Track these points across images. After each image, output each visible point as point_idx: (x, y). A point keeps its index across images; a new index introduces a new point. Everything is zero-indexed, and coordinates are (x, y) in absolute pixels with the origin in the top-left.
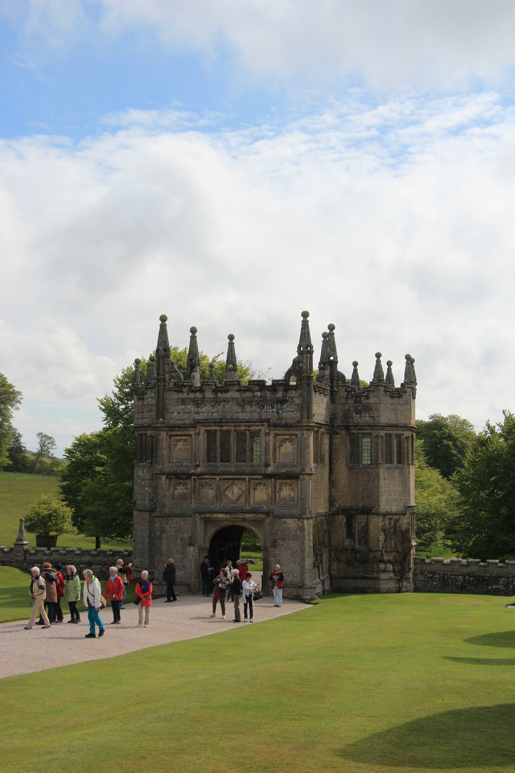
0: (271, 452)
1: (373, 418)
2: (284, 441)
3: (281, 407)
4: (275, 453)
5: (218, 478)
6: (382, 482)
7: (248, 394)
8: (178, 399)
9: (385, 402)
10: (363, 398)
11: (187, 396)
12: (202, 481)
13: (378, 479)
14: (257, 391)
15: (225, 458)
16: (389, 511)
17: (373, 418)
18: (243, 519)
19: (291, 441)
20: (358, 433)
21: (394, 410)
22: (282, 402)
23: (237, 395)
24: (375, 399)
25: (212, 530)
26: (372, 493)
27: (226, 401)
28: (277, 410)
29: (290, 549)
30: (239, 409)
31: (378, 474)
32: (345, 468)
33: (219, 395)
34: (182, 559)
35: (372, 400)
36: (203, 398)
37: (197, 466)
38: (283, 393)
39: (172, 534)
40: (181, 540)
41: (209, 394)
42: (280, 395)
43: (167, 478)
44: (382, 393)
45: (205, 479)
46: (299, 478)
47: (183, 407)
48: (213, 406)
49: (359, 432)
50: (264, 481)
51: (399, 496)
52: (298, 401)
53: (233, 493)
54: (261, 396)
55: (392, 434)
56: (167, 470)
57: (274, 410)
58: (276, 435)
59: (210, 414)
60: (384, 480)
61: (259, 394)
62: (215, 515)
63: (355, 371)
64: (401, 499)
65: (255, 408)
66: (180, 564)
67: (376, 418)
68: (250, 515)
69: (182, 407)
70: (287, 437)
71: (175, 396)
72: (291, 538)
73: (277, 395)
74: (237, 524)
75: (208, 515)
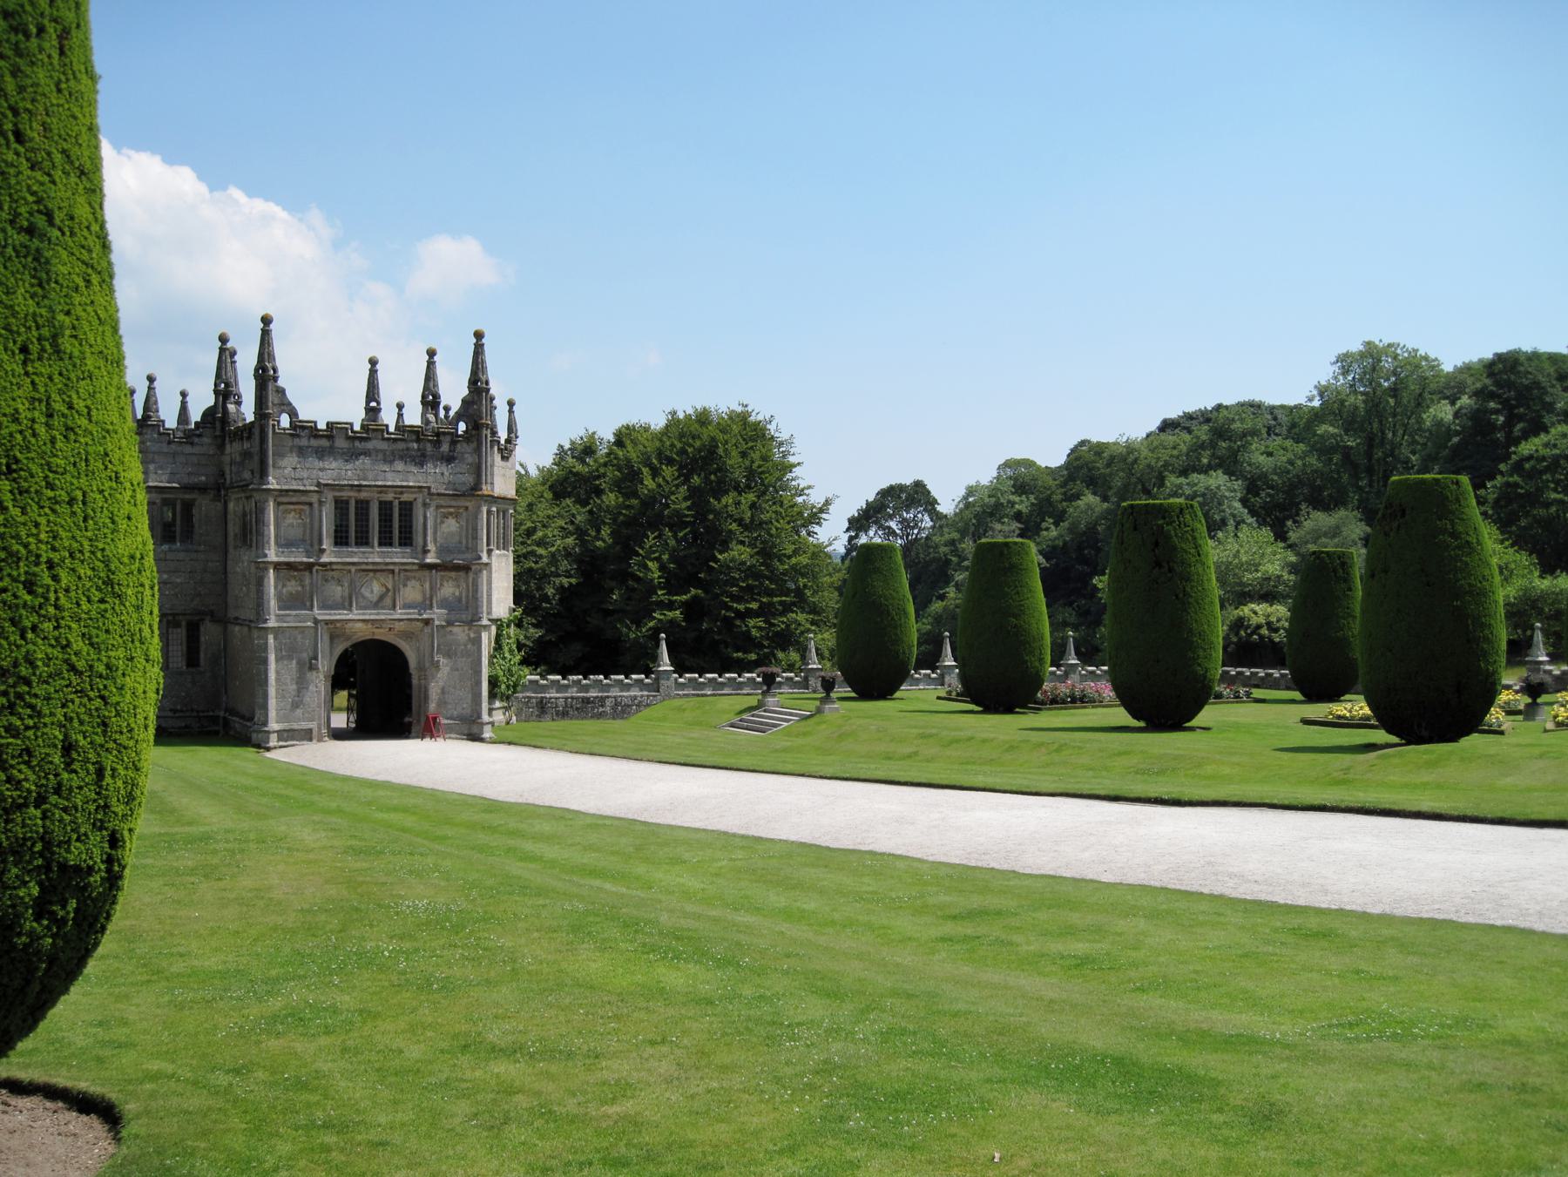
2: (446, 516)
4: (435, 533)
5: (353, 569)
19: (457, 516)
23: (383, 446)
33: (357, 443)
36: (332, 447)
37: (322, 551)
41: (341, 443)
42: (445, 448)
50: (418, 574)
52: (469, 459)
58: (438, 507)
61: (415, 445)
63: (400, 415)
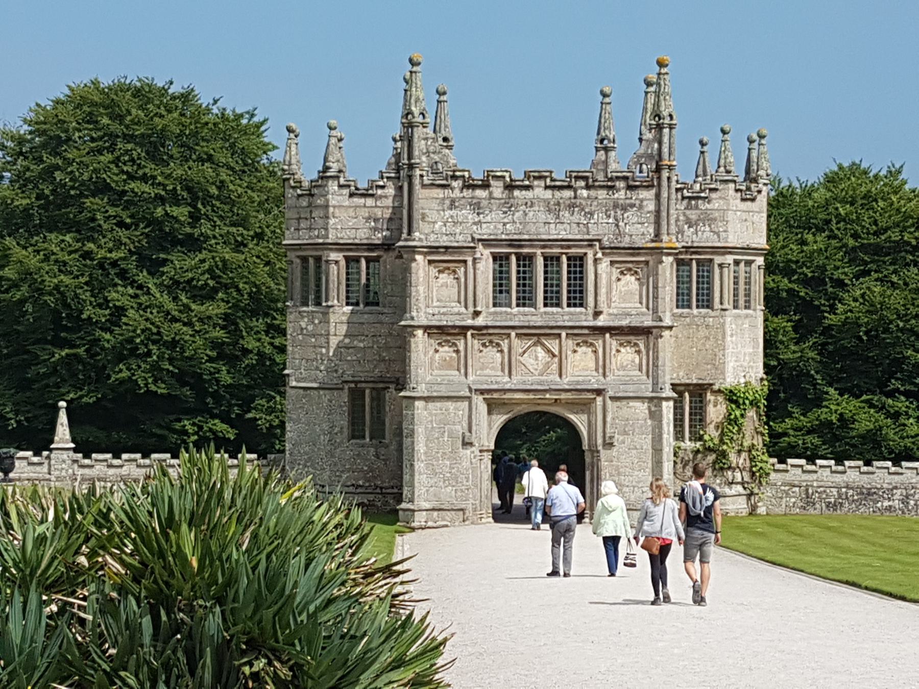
6: (729, 339)
7: (568, 193)
8: (444, 199)
10: (700, 202)
13: (724, 337)
14: (582, 188)
20: (692, 259)
23: (548, 194)
24: (722, 202)
25: (500, 420)
28: (616, 220)
30: (551, 218)
35: (715, 205)
37: (477, 314)
43: (425, 332)
44: (732, 192)
46: (651, 333)
48: (505, 213)
49: (694, 257)
53: (537, 358)
55: (742, 260)
56: (425, 322)
59: (500, 226)
60: (732, 335)
62: (508, 396)
69: (451, 212)
70: (630, 265)
71: (439, 193)
72: (637, 430)
73: (616, 196)
75: (496, 396)
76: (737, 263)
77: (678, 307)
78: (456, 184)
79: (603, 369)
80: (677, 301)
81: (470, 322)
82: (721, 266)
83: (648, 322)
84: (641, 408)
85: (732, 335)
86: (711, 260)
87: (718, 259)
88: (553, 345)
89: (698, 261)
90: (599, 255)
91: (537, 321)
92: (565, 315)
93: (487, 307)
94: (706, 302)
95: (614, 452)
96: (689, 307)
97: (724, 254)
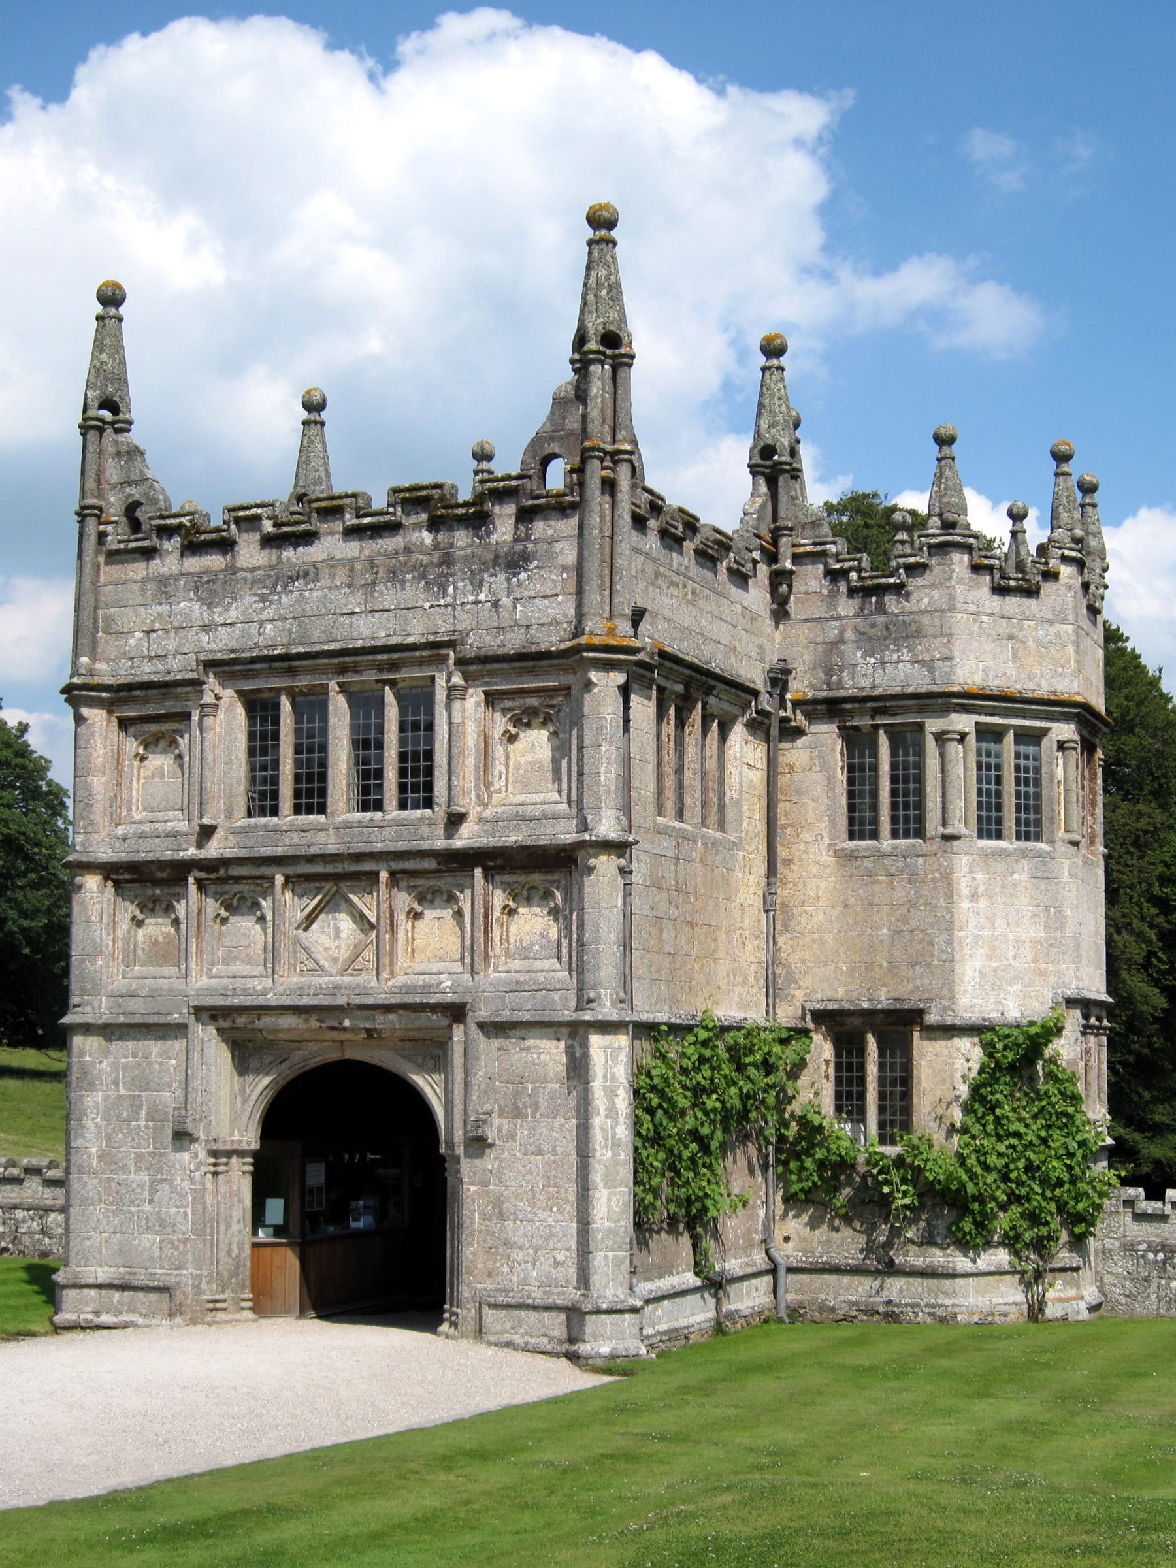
0: (470, 762)
1: (929, 665)
3: (508, 580)
6: (965, 905)
8: (145, 581)
9: (972, 608)
11: (175, 569)
12: (226, 888)
13: (950, 897)
15: (311, 797)
16: (994, 1015)
17: (929, 665)
18: (369, 1032)
20: (876, 727)
21: (1011, 637)
22: (515, 562)
23: (352, 549)
24: (935, 594)
26: (930, 944)
27: (308, 574)
29: (540, 1152)
30: (355, 602)
31: (947, 877)
32: (828, 858)
33: (288, 554)
34: (153, 1191)
36: (231, 570)
37: (207, 832)
38: (516, 527)
39: (122, 1091)
40: (150, 1117)
41: (250, 553)
43: (106, 879)
45: (238, 879)
46: (575, 862)
47: (164, 608)
48: (263, 598)
50: (444, 883)
51: (1035, 960)
53: (337, 933)
54: (436, 546)
55: (1007, 727)
56: (105, 854)
57: (482, 597)
60: (974, 896)
61: (427, 537)
62: (267, 1021)
64: (1042, 974)
65: (414, 593)
66: (147, 1207)
67: (938, 663)
68: (392, 1017)
69: (159, 609)
70: (533, 701)
71: (138, 570)
72: (543, 1105)
73: (494, 538)
74: (350, 1054)
75: (241, 1021)
76: (984, 732)
77: (851, 836)
78: (171, 545)
79: (475, 955)
80: (851, 821)
81: (192, 852)
82: (941, 738)
83: (566, 834)
84: (551, 1053)
85: (974, 896)
86: (920, 727)
87: (933, 725)
88: (367, 904)
89: (891, 731)
90: (457, 679)
91: (332, 844)
92: (395, 826)
93: (229, 814)
94: (910, 820)
95: (489, 1162)
96: (875, 835)
97: (945, 711)
